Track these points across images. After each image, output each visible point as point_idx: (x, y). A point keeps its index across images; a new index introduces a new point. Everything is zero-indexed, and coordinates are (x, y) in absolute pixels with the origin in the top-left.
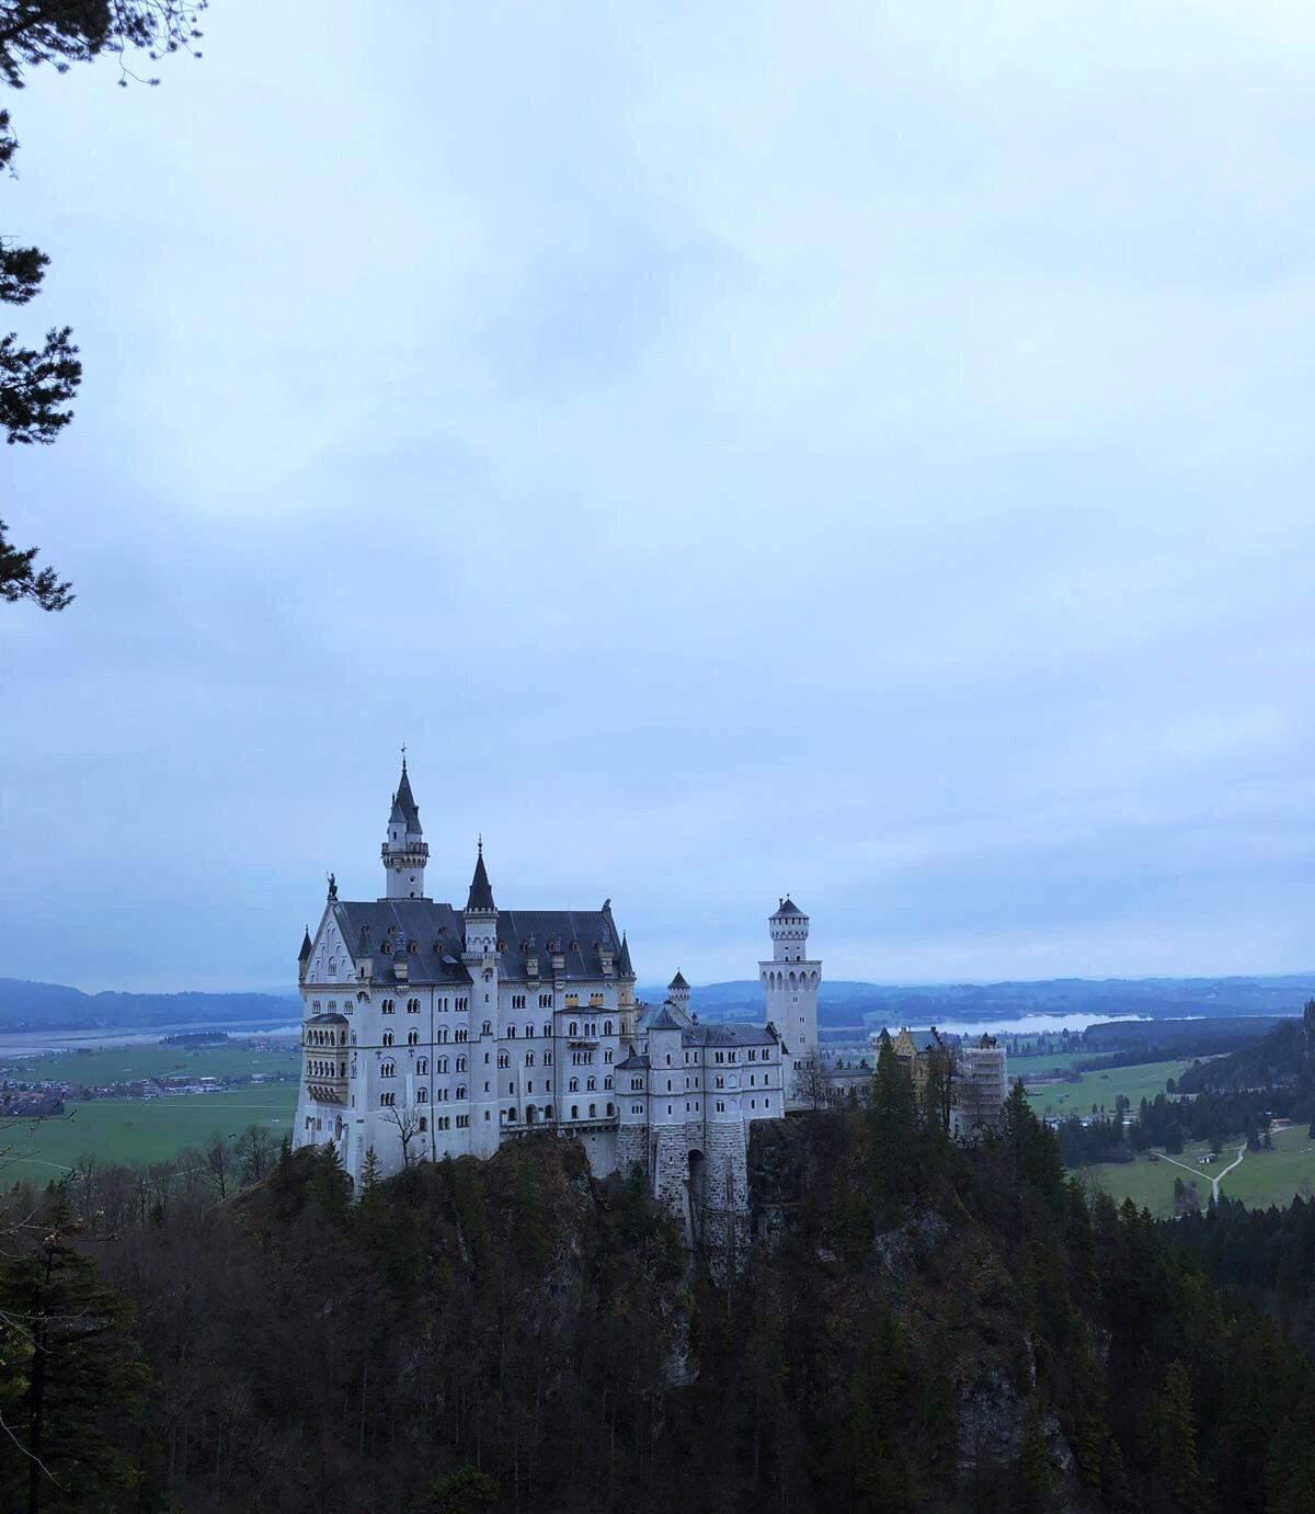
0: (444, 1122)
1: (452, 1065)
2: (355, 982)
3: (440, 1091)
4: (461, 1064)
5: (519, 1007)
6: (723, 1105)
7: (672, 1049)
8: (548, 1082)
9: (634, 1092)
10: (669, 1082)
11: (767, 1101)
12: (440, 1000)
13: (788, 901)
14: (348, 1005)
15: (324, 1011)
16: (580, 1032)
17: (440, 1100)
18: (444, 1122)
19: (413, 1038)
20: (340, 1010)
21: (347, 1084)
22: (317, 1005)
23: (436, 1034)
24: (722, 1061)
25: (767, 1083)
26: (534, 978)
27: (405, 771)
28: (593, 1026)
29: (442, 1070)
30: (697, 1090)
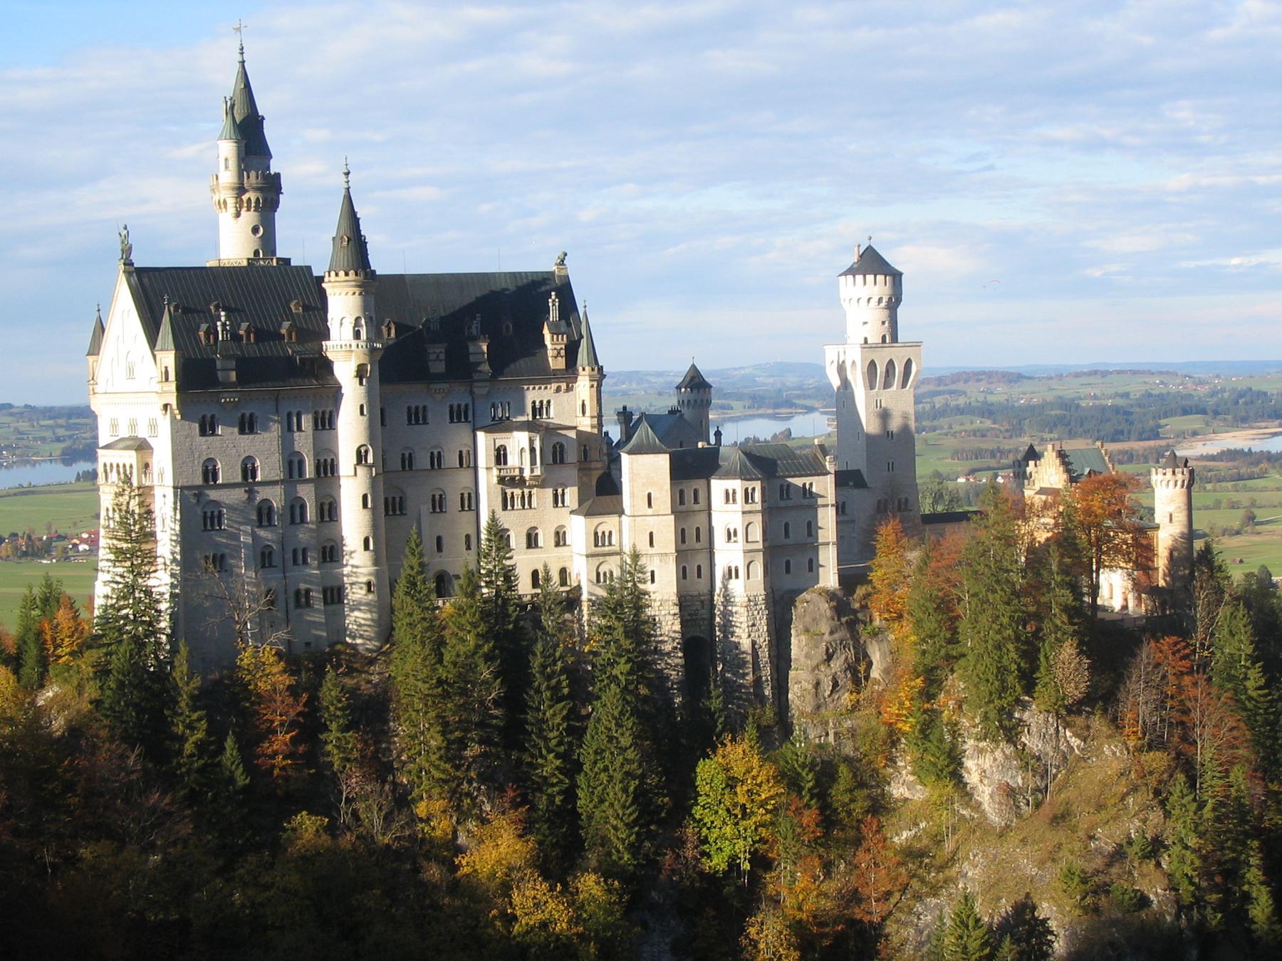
3: (295, 551)
4: (329, 511)
8: (468, 537)
9: (599, 550)
10: (651, 534)
13: (870, 250)
14: (153, 426)
15: (124, 432)
16: (513, 460)
17: (295, 562)
19: (248, 470)
20: (142, 433)
22: (114, 426)
24: (734, 500)
26: (439, 378)
29: (298, 520)
30: (698, 546)
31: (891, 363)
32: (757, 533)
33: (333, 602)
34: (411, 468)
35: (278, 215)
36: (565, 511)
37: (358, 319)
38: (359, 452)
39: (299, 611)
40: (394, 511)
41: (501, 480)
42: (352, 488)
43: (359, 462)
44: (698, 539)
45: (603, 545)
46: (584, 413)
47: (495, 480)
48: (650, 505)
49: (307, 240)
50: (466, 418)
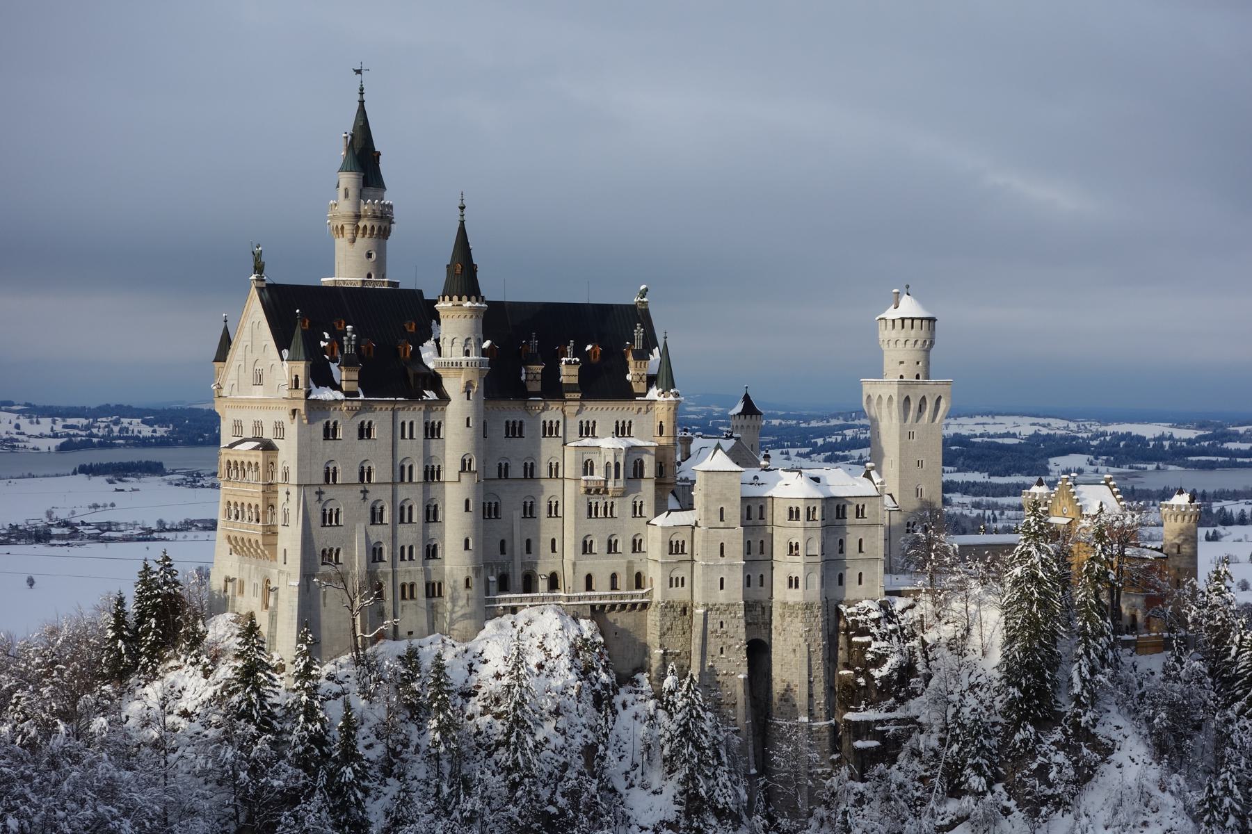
0: (407, 589)
1: (417, 515)
2: (287, 394)
4: (432, 514)
5: (514, 436)
6: (797, 579)
7: (727, 500)
8: (553, 541)
11: (860, 574)
12: (403, 424)
14: (279, 427)
16: (599, 475)
18: (407, 589)
19: (365, 475)
20: (268, 434)
21: (275, 534)
22: (238, 425)
23: (398, 469)
24: (798, 518)
25: (860, 551)
27: (362, 102)
28: (617, 465)
29: (406, 520)
30: (761, 557)
31: (924, 399)
32: (816, 549)
33: (434, 596)
34: (506, 478)
35: (390, 242)
36: (644, 520)
37: (468, 339)
38: (464, 461)
39: (404, 602)
40: (490, 514)
41: (588, 491)
42: (455, 496)
43: (463, 470)
44: (762, 552)
45: (677, 553)
46: (661, 433)
47: (583, 490)
48: (722, 519)
49: (418, 266)
50: (557, 432)
